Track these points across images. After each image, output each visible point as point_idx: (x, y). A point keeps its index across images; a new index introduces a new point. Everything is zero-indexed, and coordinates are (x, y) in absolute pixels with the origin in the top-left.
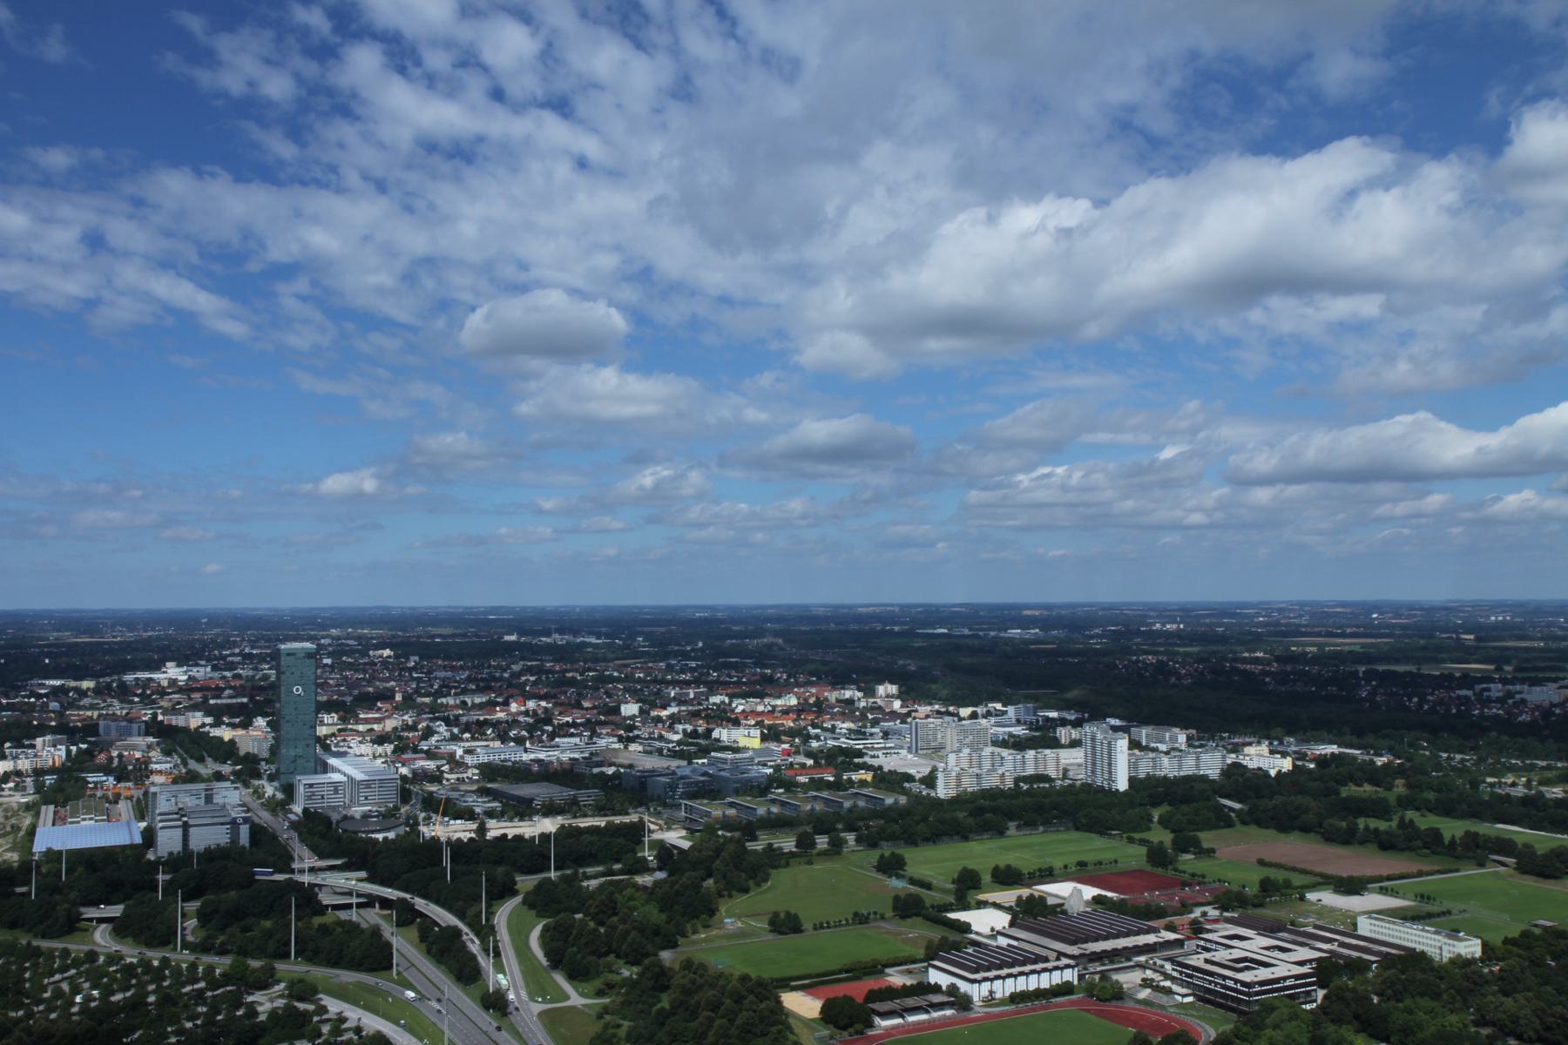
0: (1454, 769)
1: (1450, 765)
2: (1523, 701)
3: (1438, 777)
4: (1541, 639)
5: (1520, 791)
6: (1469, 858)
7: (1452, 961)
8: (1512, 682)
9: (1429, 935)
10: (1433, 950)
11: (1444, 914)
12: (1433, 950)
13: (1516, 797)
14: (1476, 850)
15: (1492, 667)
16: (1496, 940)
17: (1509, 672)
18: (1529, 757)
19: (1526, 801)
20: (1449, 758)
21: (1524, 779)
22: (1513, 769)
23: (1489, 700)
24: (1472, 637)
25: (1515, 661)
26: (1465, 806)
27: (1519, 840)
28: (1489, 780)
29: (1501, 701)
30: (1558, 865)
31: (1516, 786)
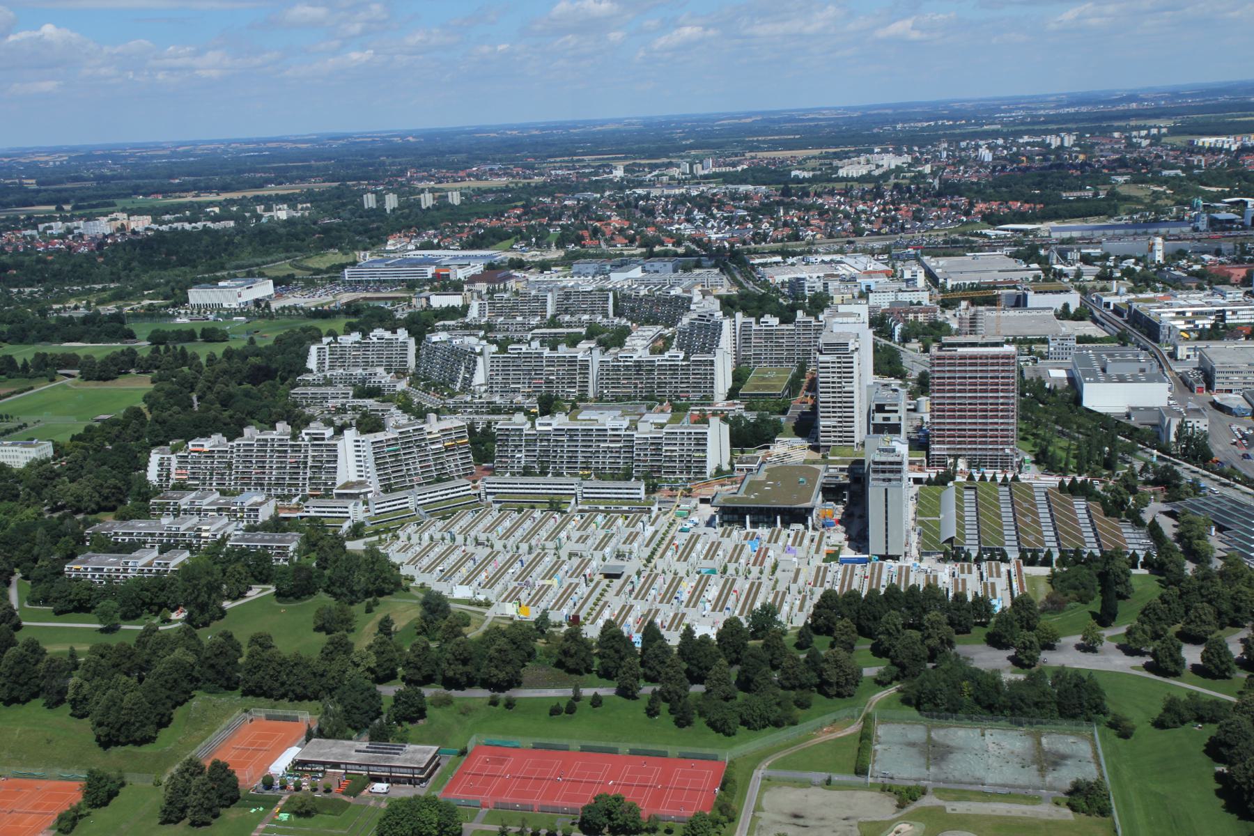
0: (24, 301)
1: (20, 298)
2: (81, 236)
3: (9, 310)
4: (93, 180)
5: (82, 312)
6: (41, 376)
7: (29, 465)
8: (70, 219)
9: (7, 448)
10: (12, 460)
11: (20, 427)
12: (12, 460)
13: (78, 318)
14: (46, 368)
15: (53, 208)
16: (65, 439)
17: (68, 212)
18: (88, 283)
19: (86, 320)
20: (19, 292)
21: (84, 302)
22: (73, 295)
23: (52, 237)
24: (34, 181)
25: (72, 201)
26: (34, 333)
27: (81, 354)
28: (55, 307)
29: (62, 236)
30: (112, 368)
31: (76, 309)
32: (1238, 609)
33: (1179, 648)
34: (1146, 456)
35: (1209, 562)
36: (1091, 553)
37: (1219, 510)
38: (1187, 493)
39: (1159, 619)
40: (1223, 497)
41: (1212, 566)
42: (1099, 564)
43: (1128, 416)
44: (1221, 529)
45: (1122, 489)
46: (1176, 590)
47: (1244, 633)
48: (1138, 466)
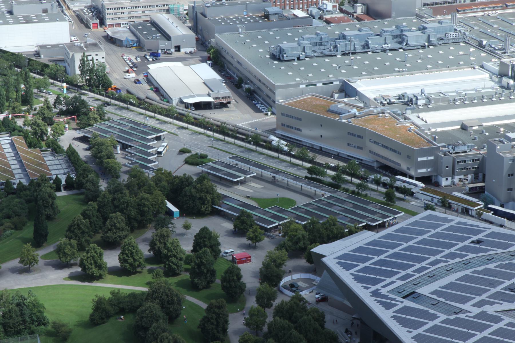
32: (142, 213)
33: (101, 255)
34: (56, 89)
35: (118, 177)
36: (20, 183)
37: (121, 131)
38: (95, 119)
39: (83, 233)
40: (123, 119)
41: (121, 180)
42: (28, 192)
43: (37, 54)
44: (124, 147)
45: (40, 122)
46: (95, 205)
47: (149, 233)
48: (52, 99)
